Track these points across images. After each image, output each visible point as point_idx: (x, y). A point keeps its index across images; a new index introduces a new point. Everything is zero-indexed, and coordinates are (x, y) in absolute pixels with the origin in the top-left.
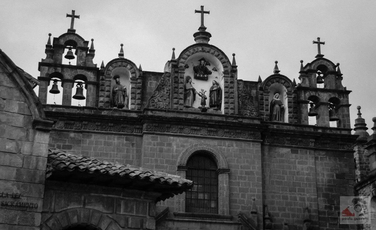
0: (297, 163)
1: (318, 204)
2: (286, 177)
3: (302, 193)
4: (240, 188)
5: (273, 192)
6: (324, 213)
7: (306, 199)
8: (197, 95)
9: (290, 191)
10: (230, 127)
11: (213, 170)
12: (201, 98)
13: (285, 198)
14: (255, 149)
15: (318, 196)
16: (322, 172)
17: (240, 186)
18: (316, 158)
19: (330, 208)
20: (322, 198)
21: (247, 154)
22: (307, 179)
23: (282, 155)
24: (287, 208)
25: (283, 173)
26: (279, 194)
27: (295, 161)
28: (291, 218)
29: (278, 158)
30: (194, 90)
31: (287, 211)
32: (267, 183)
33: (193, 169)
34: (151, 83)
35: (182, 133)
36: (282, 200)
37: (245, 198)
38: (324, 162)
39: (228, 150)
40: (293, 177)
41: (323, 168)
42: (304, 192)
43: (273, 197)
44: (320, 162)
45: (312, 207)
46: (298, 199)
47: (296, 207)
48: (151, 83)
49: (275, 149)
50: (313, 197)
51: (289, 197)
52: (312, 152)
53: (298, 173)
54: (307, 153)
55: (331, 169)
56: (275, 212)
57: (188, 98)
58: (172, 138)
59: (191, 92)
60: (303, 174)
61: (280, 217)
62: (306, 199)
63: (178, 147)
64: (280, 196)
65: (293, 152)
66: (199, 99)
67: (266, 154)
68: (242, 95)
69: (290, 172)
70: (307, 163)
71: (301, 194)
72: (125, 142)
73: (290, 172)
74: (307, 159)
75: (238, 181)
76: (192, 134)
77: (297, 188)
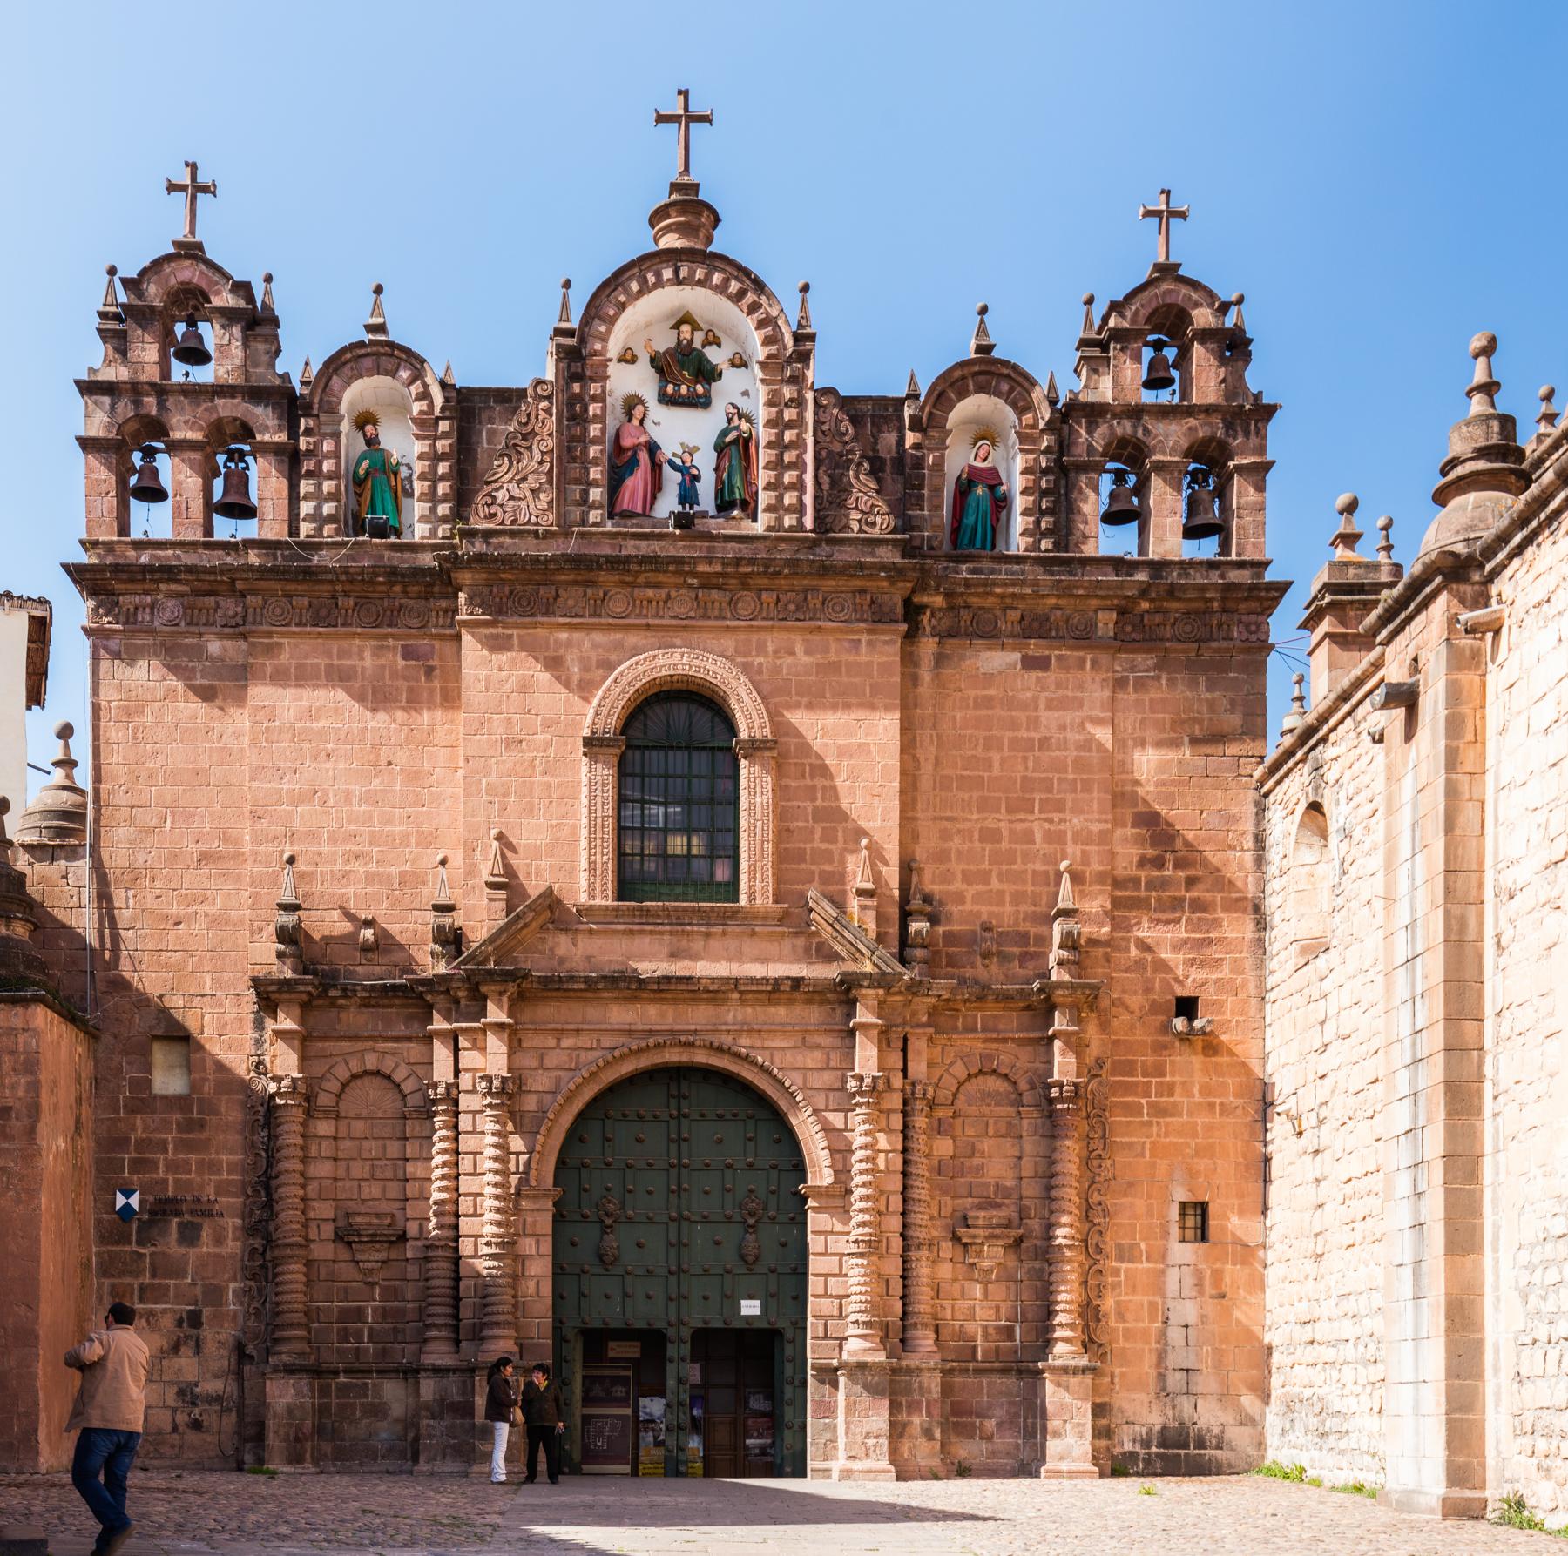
0: (1042, 706)
1: (1112, 854)
2: (996, 757)
3: (1056, 816)
4: (815, 808)
5: (948, 819)
6: (1136, 881)
7: (1069, 835)
8: (666, 468)
9: (1009, 811)
10: (787, 582)
11: (720, 749)
12: (678, 477)
13: (991, 836)
14: (877, 659)
15: (1116, 823)
16: (1138, 733)
17: (819, 803)
18: (1120, 684)
19: (1159, 863)
20: (1130, 831)
21: (845, 679)
22: (1080, 765)
23: (989, 678)
24: (994, 875)
25: (987, 747)
26: (967, 825)
27: (1035, 699)
28: (1008, 908)
29: (972, 693)
30: (653, 448)
31: (995, 884)
32: (925, 783)
33: (647, 747)
34: (492, 433)
35: (600, 616)
36: (977, 845)
37: (834, 841)
38: (1146, 697)
39: (778, 670)
40: (1025, 759)
41: (1143, 721)
42: (1061, 810)
43: (945, 835)
44: (1133, 696)
45: (1088, 864)
46: (1038, 837)
47: (1030, 866)
48: (492, 433)
49: (962, 658)
50: (1096, 827)
51: (1005, 833)
52: (1104, 658)
53: (1044, 742)
54: (1082, 666)
55: (1173, 721)
56: (952, 888)
57: (630, 482)
58: (564, 635)
59: (644, 456)
60: (1063, 745)
61: (968, 907)
62: (1069, 835)
63: (586, 669)
64: (971, 831)
65: (1030, 663)
66: (672, 479)
67: (926, 676)
68: (830, 453)
69: (1014, 743)
70: (1081, 706)
71: (1051, 821)
72: (401, 663)
73: (1014, 743)
74: (1080, 686)
75: (808, 782)
76: (638, 616)
77: (1038, 796)
